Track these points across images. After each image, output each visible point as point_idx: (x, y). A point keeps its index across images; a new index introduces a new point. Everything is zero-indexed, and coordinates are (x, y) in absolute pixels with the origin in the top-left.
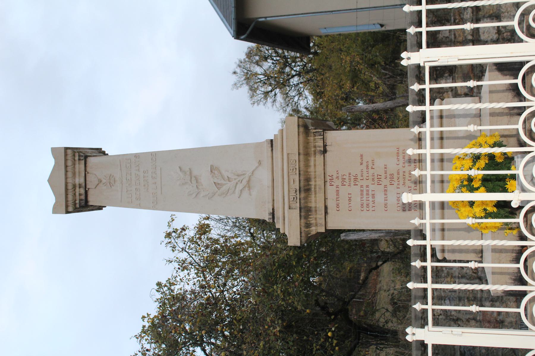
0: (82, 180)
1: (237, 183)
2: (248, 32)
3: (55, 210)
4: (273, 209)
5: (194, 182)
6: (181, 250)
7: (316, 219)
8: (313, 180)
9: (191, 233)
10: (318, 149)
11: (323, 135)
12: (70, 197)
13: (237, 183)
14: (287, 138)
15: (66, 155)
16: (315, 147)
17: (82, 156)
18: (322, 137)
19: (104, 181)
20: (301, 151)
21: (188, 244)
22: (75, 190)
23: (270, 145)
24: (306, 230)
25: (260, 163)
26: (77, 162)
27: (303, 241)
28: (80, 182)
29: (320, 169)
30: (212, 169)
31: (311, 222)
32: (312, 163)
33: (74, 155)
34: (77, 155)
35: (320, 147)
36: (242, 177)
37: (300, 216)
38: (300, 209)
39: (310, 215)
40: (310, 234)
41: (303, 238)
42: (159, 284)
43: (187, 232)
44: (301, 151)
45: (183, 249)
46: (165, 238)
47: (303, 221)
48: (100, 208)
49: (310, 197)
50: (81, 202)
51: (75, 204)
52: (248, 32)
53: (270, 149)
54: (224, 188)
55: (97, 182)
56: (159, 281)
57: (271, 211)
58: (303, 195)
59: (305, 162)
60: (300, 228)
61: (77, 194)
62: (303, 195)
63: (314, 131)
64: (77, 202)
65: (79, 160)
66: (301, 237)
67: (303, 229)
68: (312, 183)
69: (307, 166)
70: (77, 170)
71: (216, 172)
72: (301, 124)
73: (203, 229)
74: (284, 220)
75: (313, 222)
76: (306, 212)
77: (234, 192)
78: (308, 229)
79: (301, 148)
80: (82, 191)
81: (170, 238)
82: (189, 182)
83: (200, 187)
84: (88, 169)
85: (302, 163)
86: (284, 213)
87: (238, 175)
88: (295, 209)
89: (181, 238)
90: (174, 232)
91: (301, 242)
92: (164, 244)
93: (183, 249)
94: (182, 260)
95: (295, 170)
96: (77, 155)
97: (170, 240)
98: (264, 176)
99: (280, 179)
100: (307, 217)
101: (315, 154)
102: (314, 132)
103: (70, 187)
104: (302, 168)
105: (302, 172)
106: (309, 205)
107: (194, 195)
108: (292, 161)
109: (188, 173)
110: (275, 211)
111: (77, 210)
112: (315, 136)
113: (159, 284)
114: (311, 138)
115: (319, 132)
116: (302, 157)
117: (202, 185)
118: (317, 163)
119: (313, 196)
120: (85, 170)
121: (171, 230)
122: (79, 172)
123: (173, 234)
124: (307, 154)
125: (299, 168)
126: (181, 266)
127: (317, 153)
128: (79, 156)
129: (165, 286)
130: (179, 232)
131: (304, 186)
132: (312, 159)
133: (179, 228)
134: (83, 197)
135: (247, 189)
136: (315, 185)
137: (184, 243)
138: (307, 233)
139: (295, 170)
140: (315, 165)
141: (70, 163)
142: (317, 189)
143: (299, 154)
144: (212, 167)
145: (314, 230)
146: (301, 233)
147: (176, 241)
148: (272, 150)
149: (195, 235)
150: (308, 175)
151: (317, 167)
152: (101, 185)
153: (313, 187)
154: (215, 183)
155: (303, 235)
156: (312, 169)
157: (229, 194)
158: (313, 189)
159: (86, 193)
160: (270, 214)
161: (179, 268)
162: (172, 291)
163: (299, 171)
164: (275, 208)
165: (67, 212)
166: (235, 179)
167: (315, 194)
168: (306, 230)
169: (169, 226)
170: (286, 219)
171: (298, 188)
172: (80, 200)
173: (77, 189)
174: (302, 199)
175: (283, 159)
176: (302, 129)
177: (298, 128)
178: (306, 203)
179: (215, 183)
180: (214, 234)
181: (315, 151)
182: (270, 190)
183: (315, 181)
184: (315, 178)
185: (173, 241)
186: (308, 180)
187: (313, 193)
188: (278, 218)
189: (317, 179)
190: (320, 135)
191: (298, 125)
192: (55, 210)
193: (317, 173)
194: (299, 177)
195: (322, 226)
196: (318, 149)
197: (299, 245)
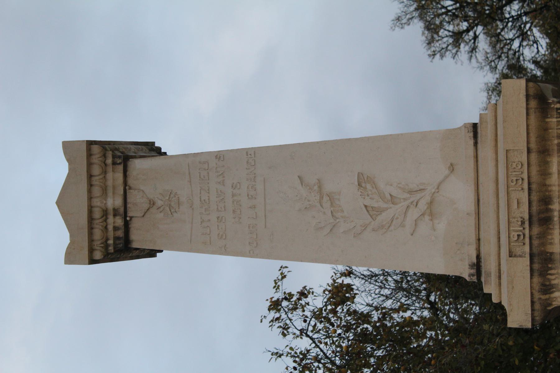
0: (119, 202)
3: (71, 258)
4: (478, 257)
6: (298, 333)
9: (317, 301)
12: (98, 234)
14: (504, 121)
15: (89, 155)
19: (159, 203)
20: (533, 146)
21: (313, 323)
22: (106, 220)
23: (471, 134)
24: (543, 297)
25: (452, 168)
26: (110, 169)
27: (537, 318)
28: (118, 205)
30: (363, 182)
31: (553, 282)
33: (105, 156)
34: (110, 154)
36: (418, 196)
37: (532, 270)
38: (532, 256)
39: (551, 269)
40: (550, 305)
41: (536, 314)
43: (309, 299)
44: (533, 146)
45: (303, 332)
46: (269, 310)
47: (536, 280)
48: (152, 253)
49: (551, 234)
50: (118, 242)
51: (107, 246)
53: (472, 142)
54: (384, 217)
55: (146, 206)
57: (475, 260)
58: (536, 230)
60: (532, 294)
61: (110, 228)
62: (536, 230)
64: (111, 242)
65: (114, 163)
66: (533, 310)
67: (537, 296)
69: (545, 173)
70: (110, 183)
71: (369, 186)
72: (532, 92)
73: (340, 294)
77: (402, 225)
79: (533, 139)
80: (119, 222)
81: (279, 311)
82: (318, 205)
83: (339, 215)
84: (130, 182)
86: (500, 265)
87: (411, 192)
88: (520, 256)
89: (299, 312)
90: (286, 299)
92: (266, 322)
93: (303, 332)
94: (301, 353)
95: (520, 182)
96: (110, 154)
97: (277, 315)
98: (459, 192)
99: (492, 200)
103: (97, 214)
104: (535, 177)
105: (534, 186)
106: (550, 249)
108: (514, 166)
109: (316, 188)
110: (482, 260)
111: (109, 257)
116: (534, 157)
117: (342, 211)
121: (279, 295)
122: (114, 187)
123: (285, 303)
125: (529, 177)
126: (299, 365)
128: (114, 157)
130: (295, 298)
133: (294, 292)
134: (120, 233)
135: (427, 218)
137: (305, 321)
138: (546, 304)
139: (520, 182)
141: (96, 170)
143: (529, 151)
144: (360, 175)
146: (533, 303)
147: (290, 316)
148: (476, 144)
149: (326, 305)
150: (546, 191)
154: (366, 206)
155: (537, 306)
157: (392, 228)
160: (472, 266)
163: (529, 184)
164: (482, 255)
165: (92, 261)
166: (405, 199)
168: (543, 297)
171: (526, 216)
172: (116, 238)
173: (111, 219)
174: (534, 237)
175: (497, 161)
176: (533, 104)
177: (527, 100)
178: (543, 244)
179: (366, 206)
180: (361, 304)
182: (472, 221)
185: (284, 316)
186: (546, 201)
188: (489, 275)
191: (528, 96)
192: (71, 258)
194: (529, 195)
197: (529, 325)
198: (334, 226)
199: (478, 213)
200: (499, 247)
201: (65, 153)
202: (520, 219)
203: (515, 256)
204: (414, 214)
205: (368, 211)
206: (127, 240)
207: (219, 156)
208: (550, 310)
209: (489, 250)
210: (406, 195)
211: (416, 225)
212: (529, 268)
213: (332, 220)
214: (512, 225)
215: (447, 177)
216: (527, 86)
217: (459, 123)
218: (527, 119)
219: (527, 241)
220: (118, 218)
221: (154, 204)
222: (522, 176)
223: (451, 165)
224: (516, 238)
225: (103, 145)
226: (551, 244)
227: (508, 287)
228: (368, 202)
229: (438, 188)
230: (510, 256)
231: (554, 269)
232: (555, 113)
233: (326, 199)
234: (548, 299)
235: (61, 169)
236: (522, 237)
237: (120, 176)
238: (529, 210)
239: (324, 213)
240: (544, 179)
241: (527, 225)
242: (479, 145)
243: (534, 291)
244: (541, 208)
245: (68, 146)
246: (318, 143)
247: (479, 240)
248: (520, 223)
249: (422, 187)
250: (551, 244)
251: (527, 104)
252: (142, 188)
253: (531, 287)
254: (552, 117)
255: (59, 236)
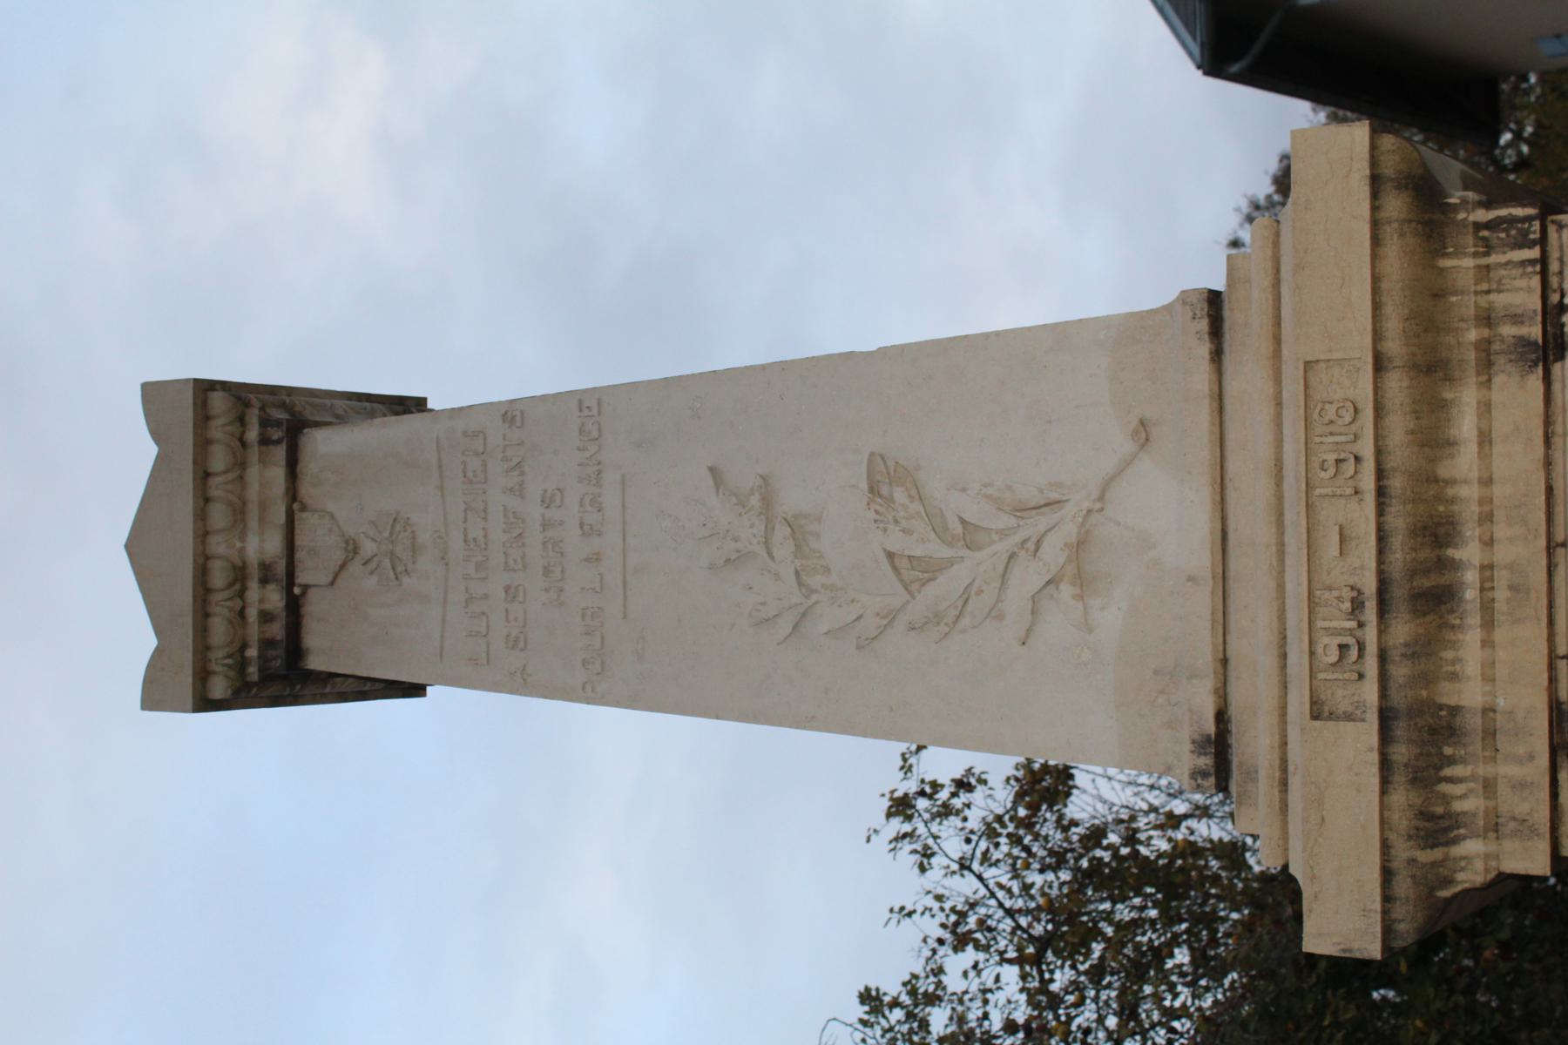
1: (1012, 556)
2: (1257, 48)
3: (154, 697)
4: (1221, 717)
5: (784, 550)
6: (955, 867)
7: (1489, 786)
8: (1471, 531)
9: (995, 798)
10: (1508, 330)
11: (1543, 241)
12: (219, 630)
13: (1012, 556)
14: (1299, 267)
15: (203, 417)
16: (1487, 319)
17: (278, 423)
18: (1535, 253)
19: (368, 547)
20: (1394, 346)
21: (983, 845)
22: (241, 594)
23: (1204, 325)
25: (1143, 433)
26: (254, 454)
27: (1402, 927)
29: (1517, 463)
30: (884, 480)
31: (1458, 806)
32: (1466, 426)
33: (242, 420)
35: (1517, 319)
36: (1043, 521)
37: (1385, 765)
38: (1386, 718)
39: (1452, 761)
40: (1448, 881)
41: (1399, 911)
42: (871, 999)
43: (978, 796)
44: (1394, 346)
45: (964, 865)
46: (889, 815)
48: (416, 690)
49: (1454, 645)
50: (271, 653)
52: (1257, 48)
53: (1204, 349)
55: (338, 556)
56: (873, 986)
57: (1211, 728)
58: (1402, 630)
59: (1417, 414)
60: (1385, 847)
61: (252, 614)
62: (1402, 630)
63: (1482, 215)
64: (252, 652)
65: (265, 441)
66: (1387, 899)
67: (1402, 850)
68: (1469, 553)
69: (1433, 439)
70: (253, 493)
71: (900, 495)
72: (1390, 166)
73: (1045, 786)
74: (1284, 784)
75: (1470, 804)
76: (1421, 739)
77: (996, 614)
78: (1437, 854)
79: (1394, 324)
80: (275, 599)
81: (909, 818)
83: (816, 581)
84: (306, 490)
85: (1398, 427)
87: (1022, 510)
88: (1349, 717)
89: (954, 821)
90: (922, 793)
91: (1388, 931)
92: (882, 842)
93: (964, 865)
94: (953, 910)
95: (1349, 468)
97: (907, 828)
98: (1165, 512)
99: (1264, 533)
100: (1427, 773)
101: (1486, 364)
102: (1478, 226)
103: (219, 577)
104: (1401, 454)
105: (1396, 483)
106: (1448, 694)
107: (784, 627)
108: (1331, 411)
109: (755, 500)
110: (1233, 728)
111: (244, 695)
112: (1488, 248)
113: (871, 999)
114: (1461, 266)
115: (1512, 221)
116: (1397, 384)
117: (827, 570)
118: (1501, 424)
119: (1471, 638)
120: (293, 494)
121: (911, 786)
123: (922, 804)
124: (1432, 369)
125: (1379, 452)
126: (953, 932)
127: (1501, 361)
128: (265, 422)
129: (895, 1003)
130: (943, 795)
131: (1412, 574)
132: (1467, 397)
133: (945, 778)
134: (277, 630)
135: (1066, 590)
136: (1487, 569)
137: (968, 841)
139: (1349, 468)
140: (1485, 439)
141: (219, 460)
142: (1501, 594)
143: (1380, 364)
144: (875, 460)
145: (1474, 861)
146: (1387, 874)
147: (934, 827)
148: (1217, 355)
149: (1014, 808)
150: (1439, 498)
151: (1498, 449)
152: (355, 567)
153: (1471, 577)
154: (891, 556)
156: (1464, 463)
157: (965, 622)
158: (1470, 594)
159: (294, 606)
160: (1201, 745)
161: (941, 942)
162: (924, 1025)
163: (1380, 474)
164: (1234, 712)
165: (204, 703)
166: (1003, 534)
167: (1488, 624)
169: (907, 769)
170: (1295, 782)
171: (1370, 584)
172: (267, 644)
173: (254, 592)
174: (1395, 655)
175: (1279, 404)
176: (1396, 205)
177: (1375, 195)
178: (1426, 679)
179: (891, 556)
180: (1080, 808)
181: (1485, 350)
182: (1202, 602)
183: (1489, 543)
184: (1487, 518)
185: (922, 829)
186: (1437, 532)
187: (1474, 620)
188: (1251, 775)
189: (1501, 531)
190: (1523, 242)
191: (1376, 182)
192: (154, 697)
193: (1498, 491)
194: (1381, 510)
195: (1534, 832)
196: (1508, 330)
197: (1374, 951)
198: (804, 615)
200: (1284, 686)
202: (1347, 594)
203: (1332, 716)
204: (1027, 578)
205: (895, 569)
206: (294, 648)
207: (512, 413)
208: (1448, 901)
210: (1005, 521)
212: (1375, 757)
214: (1321, 611)
215: (1128, 463)
216: (1373, 147)
218: (1375, 257)
219: (1371, 666)
220: (271, 587)
221: (356, 551)
222: (1356, 448)
223: (1142, 423)
224: (1333, 656)
225: (240, 394)
226: (1454, 677)
227: (1305, 820)
228: (896, 542)
229: (1101, 498)
230: (1316, 716)
232: (1470, 239)
233: (781, 532)
234: (1446, 859)
235: (138, 453)
236: (1354, 653)
237: (278, 474)
238: (1381, 560)
239: (777, 576)
240: (1433, 460)
241: (1370, 613)
242: (1227, 359)
243: (1392, 836)
244: (1422, 556)
245: (152, 392)
246: (763, 367)
247: (1225, 661)
248: (1347, 606)
249: (1054, 496)
250: (1454, 677)
251: (1375, 209)
252: (331, 507)
253: (1383, 822)
254: (1460, 253)
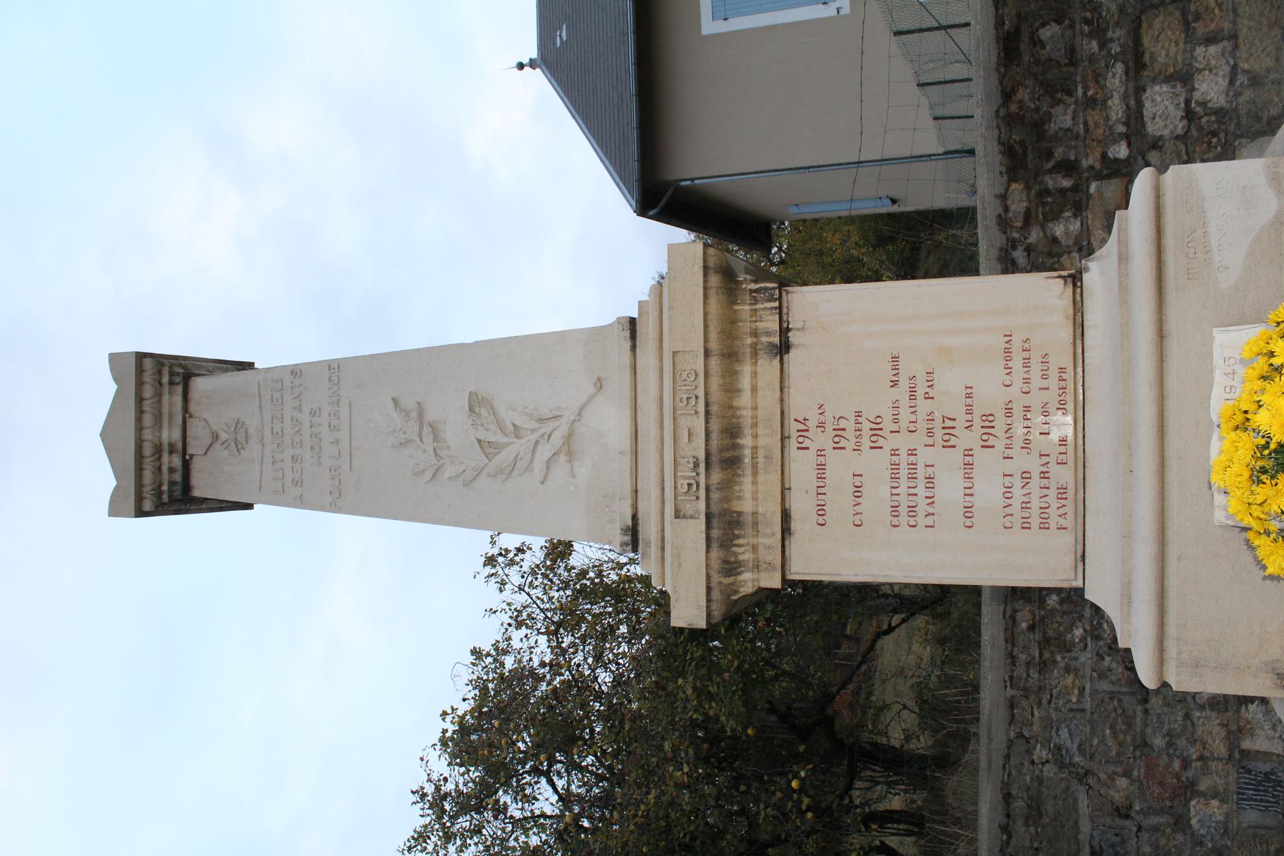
0: (177, 435)
1: (537, 442)
2: (662, 203)
3: (115, 510)
4: (635, 517)
5: (428, 438)
7: (755, 548)
8: (748, 431)
9: (536, 556)
10: (764, 339)
11: (780, 299)
12: (148, 476)
13: (537, 442)
14: (671, 308)
15: (140, 371)
16: (755, 334)
17: (178, 374)
18: (776, 304)
19: (224, 436)
20: (714, 345)
21: (530, 579)
22: (159, 459)
23: (628, 333)
24: (726, 581)
25: (599, 384)
26: (166, 390)
27: (715, 613)
28: (176, 439)
29: (768, 400)
30: (475, 404)
31: (741, 557)
32: (745, 383)
33: (160, 373)
34: (166, 371)
35: (768, 334)
36: (551, 425)
39: (738, 537)
40: (736, 592)
41: (714, 606)
42: (476, 653)
43: (528, 555)
44: (714, 345)
46: (485, 565)
47: (715, 554)
48: (249, 506)
49: (740, 484)
50: (175, 488)
51: (159, 494)
52: (662, 203)
53: (628, 344)
54: (505, 456)
55: (209, 441)
57: (629, 522)
58: (716, 476)
59: (723, 377)
60: (708, 577)
61: (165, 469)
62: (716, 476)
63: (753, 286)
64: (165, 488)
65: (171, 383)
66: (709, 601)
67: (716, 578)
68: (746, 441)
69: (731, 389)
70: (165, 410)
71: (483, 412)
72: (712, 262)
73: (559, 550)
74: (663, 548)
75: (746, 556)
76: (724, 527)
77: (529, 468)
78: (731, 579)
79: (713, 336)
80: (177, 461)
81: (494, 566)
82: (417, 438)
83: (443, 453)
84: (193, 408)
85: (715, 383)
86: (663, 530)
87: (541, 420)
88: (692, 517)
89: (516, 568)
90: (501, 554)
91: (709, 615)
93: (521, 589)
95: (693, 401)
96: (166, 371)
97: (493, 571)
98: (609, 420)
100: (727, 542)
101: (755, 355)
102: (752, 291)
103: (148, 451)
104: (716, 396)
105: (714, 409)
106: (737, 506)
107: (428, 475)
108: (685, 376)
109: (414, 414)
111: (161, 508)
112: (756, 301)
113: (476, 653)
114: (744, 309)
115: (767, 289)
116: (714, 362)
118: (761, 383)
119: (747, 480)
120: (186, 409)
121: (496, 551)
122: (171, 415)
123: (501, 559)
124: (731, 356)
125: (706, 394)
127: (761, 353)
128: (172, 374)
129: (488, 655)
130: (511, 555)
131: (722, 450)
132: (746, 369)
133: (511, 547)
134: (178, 477)
135: (563, 458)
136: (755, 448)
138: (729, 590)
139: (693, 401)
140: (754, 389)
141: (148, 392)
142: (761, 460)
143: (707, 354)
145: (748, 582)
146: (709, 589)
147: (507, 571)
148: (634, 348)
150: (733, 416)
151: (760, 393)
152: (217, 446)
153: (747, 452)
154: (479, 441)
155: (716, 595)
156: (744, 400)
157: (515, 473)
158: (747, 460)
159: (186, 465)
160: (625, 531)
161: (510, 625)
162: (502, 664)
163: (707, 404)
164: (640, 515)
165: (140, 513)
166: (533, 431)
167: (755, 474)
168: (726, 581)
169: (493, 543)
170: (668, 547)
171: (702, 456)
172: (172, 483)
173: (165, 458)
174: (713, 488)
175: (661, 371)
176: (715, 280)
177: (705, 275)
178: (727, 499)
179: (479, 441)
180: (576, 560)
181: (754, 347)
182: (627, 462)
183: (755, 436)
184: (755, 425)
185: (500, 572)
186: (732, 432)
187: (749, 472)
188: (648, 544)
189: (761, 431)
190: (771, 300)
192: (115, 510)
193: (760, 413)
194: (707, 422)
195: (774, 568)
196: (764, 339)
197: (703, 625)
198: (438, 470)
199: (635, 453)
200: (663, 503)
201: (112, 369)
202: (692, 460)
203: (684, 517)
204: (544, 452)
205: (482, 448)
206: (187, 486)
207: (296, 371)
208: (736, 601)
209: (649, 508)
210: (535, 425)
211: (548, 468)
212: (704, 535)
213: (434, 461)
214: (680, 468)
215: (592, 398)
216: (705, 253)
217: (607, 318)
218: (705, 304)
219: (702, 493)
220: (174, 455)
221: (217, 437)
222: (696, 392)
223: (599, 379)
224: (685, 489)
225: (159, 359)
226: (739, 498)
227: (672, 565)
228: (482, 435)
229: (579, 414)
230: (677, 517)
231: (743, 537)
232: (748, 297)
233: (427, 429)
236: (694, 487)
237: (178, 399)
238: (707, 445)
239: (425, 451)
240: (731, 398)
242: (638, 350)
243: (712, 572)
244: (726, 442)
245: (115, 359)
246: (419, 350)
247: (636, 491)
248: (692, 465)
249: (557, 413)
250: (739, 498)
251: (705, 281)
252: (205, 415)
253: (707, 565)
254: (743, 303)
255: (102, 479)
